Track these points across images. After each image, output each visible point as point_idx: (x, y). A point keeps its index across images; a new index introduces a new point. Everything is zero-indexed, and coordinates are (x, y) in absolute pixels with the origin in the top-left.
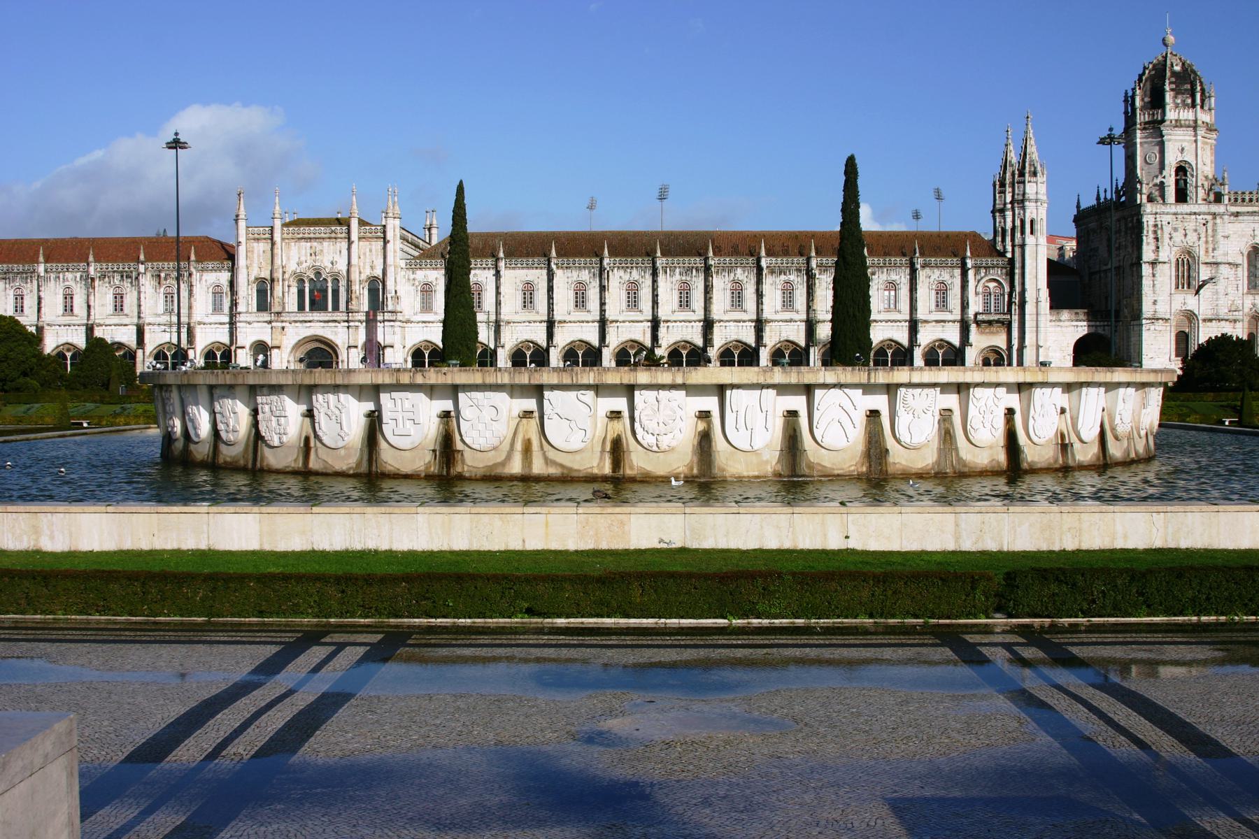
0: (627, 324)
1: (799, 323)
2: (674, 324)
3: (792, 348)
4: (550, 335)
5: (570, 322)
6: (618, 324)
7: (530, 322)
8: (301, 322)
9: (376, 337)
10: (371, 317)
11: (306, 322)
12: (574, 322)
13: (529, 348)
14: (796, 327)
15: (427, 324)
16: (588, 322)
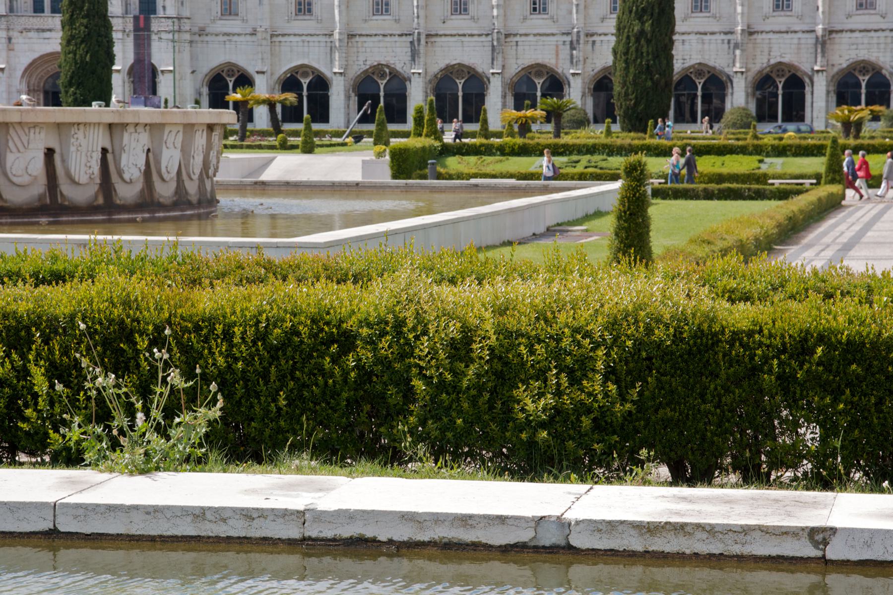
0: (531, 38)
1: (800, 35)
2: (602, 38)
3: (788, 75)
4: (414, 55)
5: (446, 35)
6: (518, 38)
7: (384, 35)
8: (38, 30)
9: (149, 55)
10: (142, 24)
11: (43, 31)
12: (451, 35)
13: (383, 76)
14: (796, 41)
15: (231, 38)
16: (472, 35)
